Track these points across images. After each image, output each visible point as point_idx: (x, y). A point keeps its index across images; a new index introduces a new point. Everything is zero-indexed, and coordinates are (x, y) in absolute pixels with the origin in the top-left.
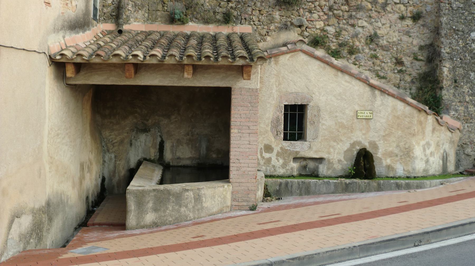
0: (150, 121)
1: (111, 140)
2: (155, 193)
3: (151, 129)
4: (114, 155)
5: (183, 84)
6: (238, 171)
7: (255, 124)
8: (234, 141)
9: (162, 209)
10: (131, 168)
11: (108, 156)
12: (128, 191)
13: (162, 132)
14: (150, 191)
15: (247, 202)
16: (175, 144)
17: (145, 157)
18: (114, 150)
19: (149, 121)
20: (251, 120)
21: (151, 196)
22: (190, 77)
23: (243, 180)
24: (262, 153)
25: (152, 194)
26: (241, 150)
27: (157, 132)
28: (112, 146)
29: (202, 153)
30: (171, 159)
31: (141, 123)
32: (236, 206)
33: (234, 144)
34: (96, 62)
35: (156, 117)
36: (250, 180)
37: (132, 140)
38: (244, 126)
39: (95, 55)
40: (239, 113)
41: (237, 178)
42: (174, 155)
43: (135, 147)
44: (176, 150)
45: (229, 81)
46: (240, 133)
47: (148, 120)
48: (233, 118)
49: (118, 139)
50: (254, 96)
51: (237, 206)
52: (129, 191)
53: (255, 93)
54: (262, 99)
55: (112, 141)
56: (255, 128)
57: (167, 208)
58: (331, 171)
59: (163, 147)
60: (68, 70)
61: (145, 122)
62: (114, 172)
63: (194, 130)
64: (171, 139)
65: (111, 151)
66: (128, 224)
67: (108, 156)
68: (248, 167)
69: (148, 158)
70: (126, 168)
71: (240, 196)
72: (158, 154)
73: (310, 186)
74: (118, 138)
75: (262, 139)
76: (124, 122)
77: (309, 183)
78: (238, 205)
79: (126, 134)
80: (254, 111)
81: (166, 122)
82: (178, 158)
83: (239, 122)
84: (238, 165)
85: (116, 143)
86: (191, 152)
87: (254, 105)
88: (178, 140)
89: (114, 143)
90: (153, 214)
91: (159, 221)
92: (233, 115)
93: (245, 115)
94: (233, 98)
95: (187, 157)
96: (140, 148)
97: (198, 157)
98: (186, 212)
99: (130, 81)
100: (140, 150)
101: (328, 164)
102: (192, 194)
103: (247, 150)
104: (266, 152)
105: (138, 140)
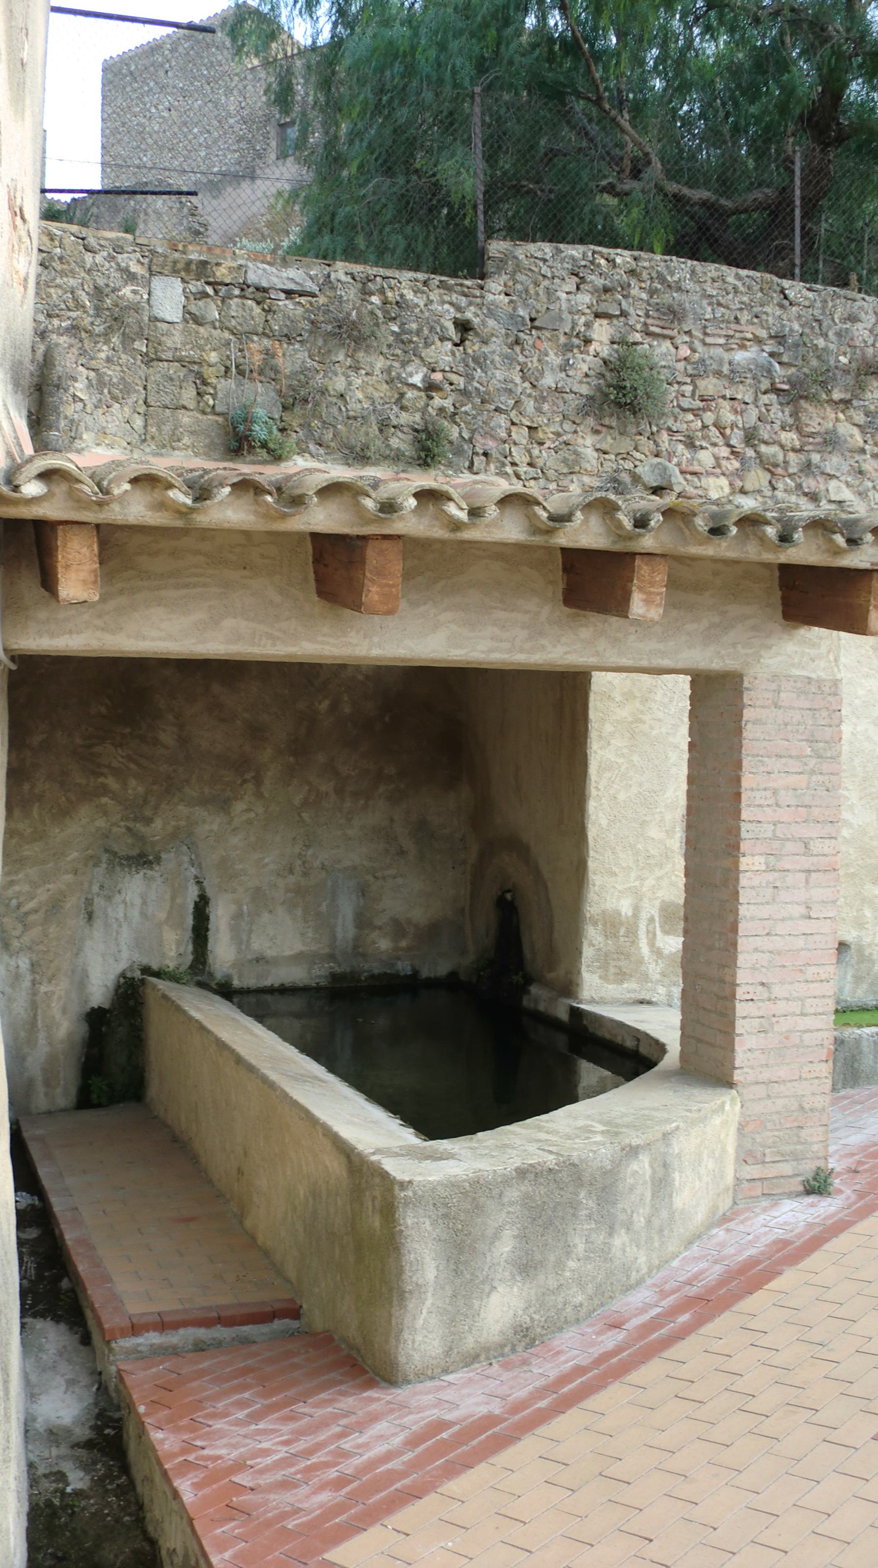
0: (158, 824)
1: (14, 902)
2: (525, 1187)
3: (164, 856)
4: (27, 961)
5: (550, 656)
6: (763, 1035)
7: (828, 829)
8: (752, 907)
9: (552, 1258)
10: (93, 1009)
11: (8, 965)
12: (410, 1193)
13: (203, 865)
14: (506, 1181)
15: (796, 1160)
16: (245, 907)
17: (145, 961)
18: (26, 939)
19: (153, 825)
20: (816, 811)
21: (511, 1203)
22: (655, 613)
23: (782, 1072)
24: (654, 934)
25: (513, 1194)
26: (777, 943)
27: (186, 865)
28: (20, 927)
29: (339, 936)
30: (234, 965)
31: (123, 830)
32: (752, 1184)
33: (752, 918)
34: (226, 525)
35: (181, 807)
36: (806, 1069)
37: (93, 900)
38: (788, 839)
39: (233, 486)
40: (771, 784)
41: (762, 1066)
42: (244, 947)
43: (107, 925)
44: (250, 931)
45: (734, 645)
46: (774, 870)
47: (148, 821)
48: (749, 806)
49: (42, 895)
50: (825, 713)
51: (759, 1183)
52: (415, 1193)
53: (830, 698)
54: (654, 732)
55: (18, 907)
56: (827, 847)
57: (568, 1249)
58: (865, 986)
59: (207, 919)
60: (67, 567)
61: (139, 827)
62: (32, 1025)
63: (310, 852)
64: (234, 891)
65: (16, 944)
66: (409, 1357)
67: (8, 965)
68: (803, 1014)
69: (155, 967)
70: (76, 1009)
71: (771, 1141)
72: (190, 948)
73: (861, 1053)
74: (39, 891)
75: (653, 882)
76: (62, 830)
77: (858, 1041)
78: (760, 1179)
79: (68, 878)
80: (827, 777)
81: (215, 827)
82: (257, 960)
83: (769, 823)
84: (766, 1008)
85: (35, 911)
86: (302, 934)
87: (825, 750)
88: (258, 889)
89: (26, 914)
90: (515, 1289)
91: (536, 1317)
92: (749, 793)
93: (791, 793)
94: (747, 721)
95: (288, 953)
96: (125, 929)
97: (327, 950)
98: (628, 1249)
99: (320, 638)
100: (126, 935)
101: (858, 963)
102: (647, 1165)
103: (800, 942)
104: (666, 932)
105: (118, 899)
